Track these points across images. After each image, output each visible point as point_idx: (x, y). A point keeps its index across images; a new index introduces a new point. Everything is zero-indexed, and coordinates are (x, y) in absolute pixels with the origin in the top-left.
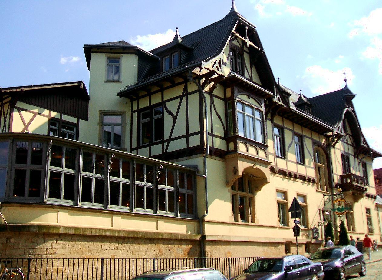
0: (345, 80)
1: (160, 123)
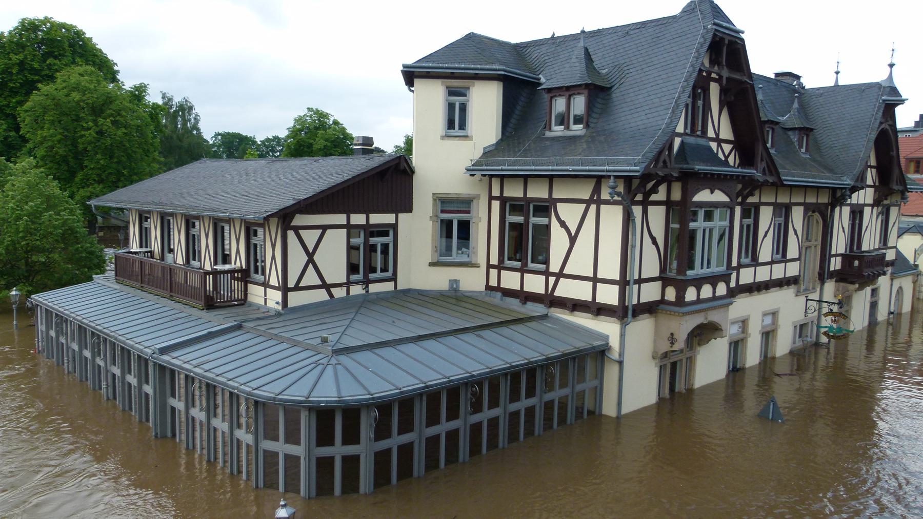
0: (891, 66)
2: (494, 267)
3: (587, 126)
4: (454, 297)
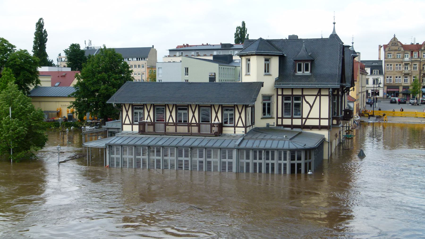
1: (299, 107)
2: (280, 118)
3: (311, 72)
4: (268, 129)
